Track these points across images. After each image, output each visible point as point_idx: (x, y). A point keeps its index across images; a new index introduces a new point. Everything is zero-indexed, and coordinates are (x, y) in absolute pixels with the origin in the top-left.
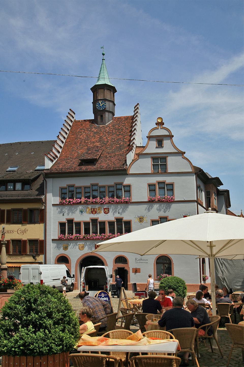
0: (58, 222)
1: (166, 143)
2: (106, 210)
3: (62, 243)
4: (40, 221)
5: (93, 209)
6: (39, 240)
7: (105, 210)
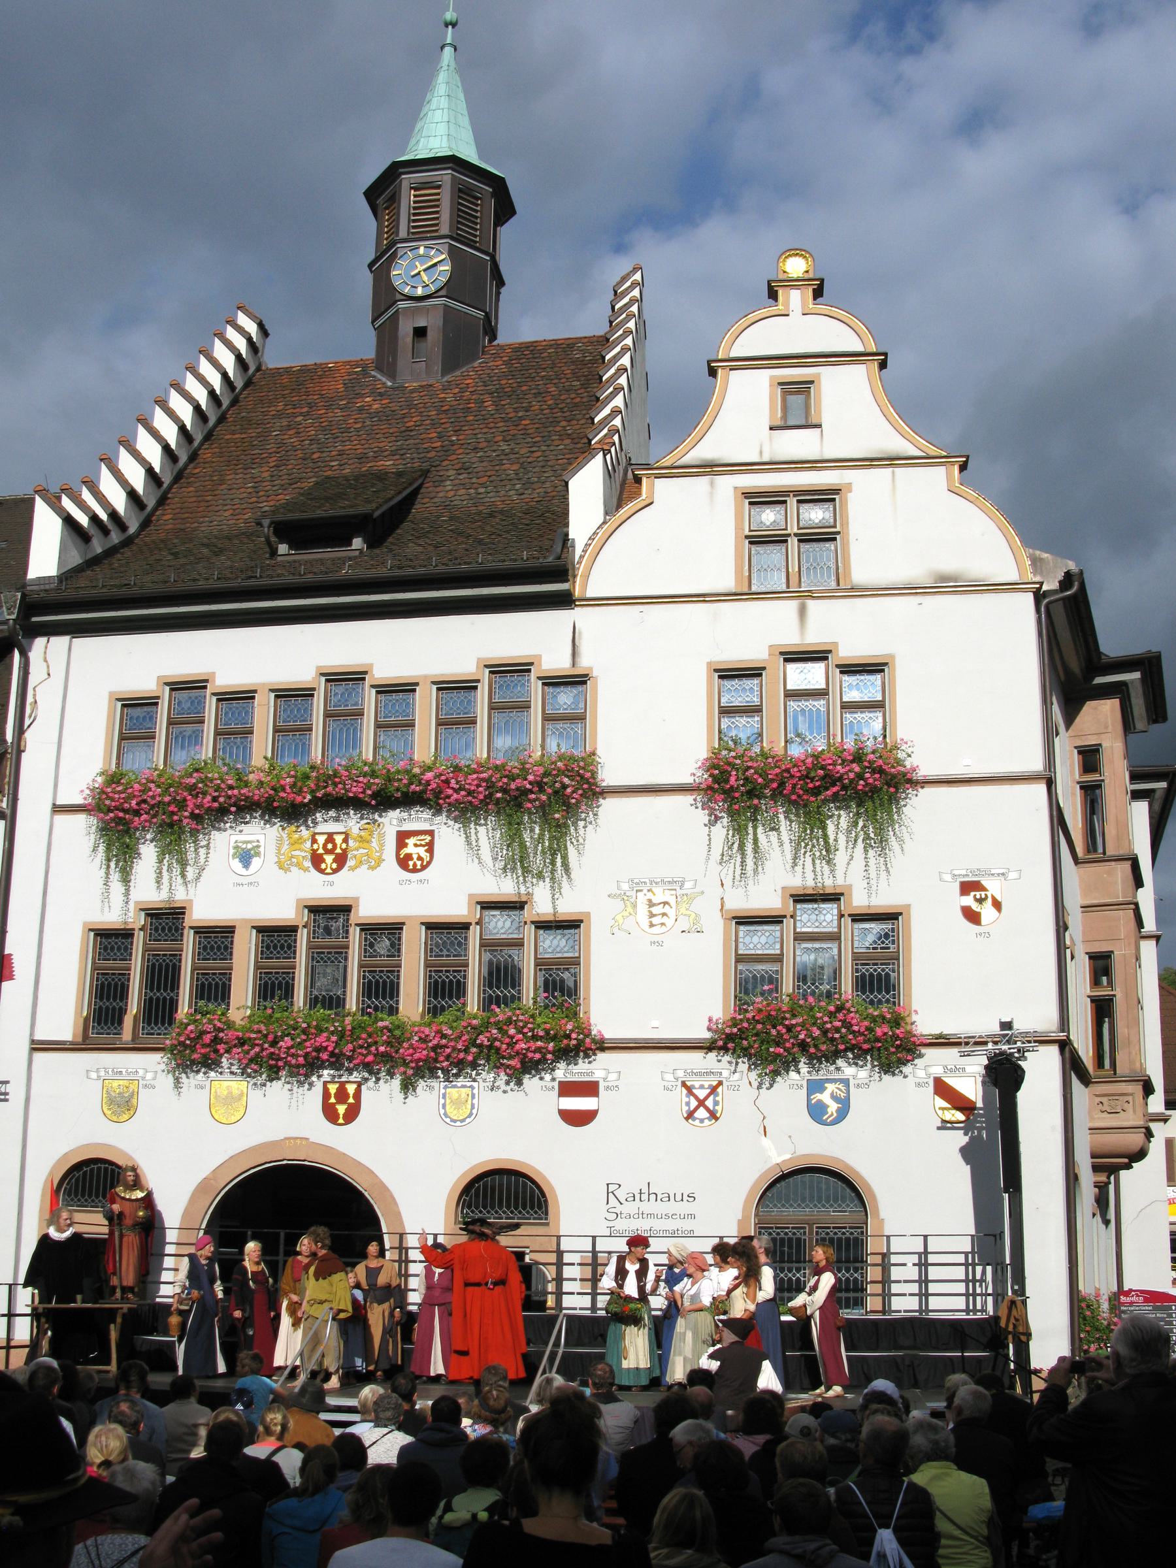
2: (411, 841)
5: (321, 839)
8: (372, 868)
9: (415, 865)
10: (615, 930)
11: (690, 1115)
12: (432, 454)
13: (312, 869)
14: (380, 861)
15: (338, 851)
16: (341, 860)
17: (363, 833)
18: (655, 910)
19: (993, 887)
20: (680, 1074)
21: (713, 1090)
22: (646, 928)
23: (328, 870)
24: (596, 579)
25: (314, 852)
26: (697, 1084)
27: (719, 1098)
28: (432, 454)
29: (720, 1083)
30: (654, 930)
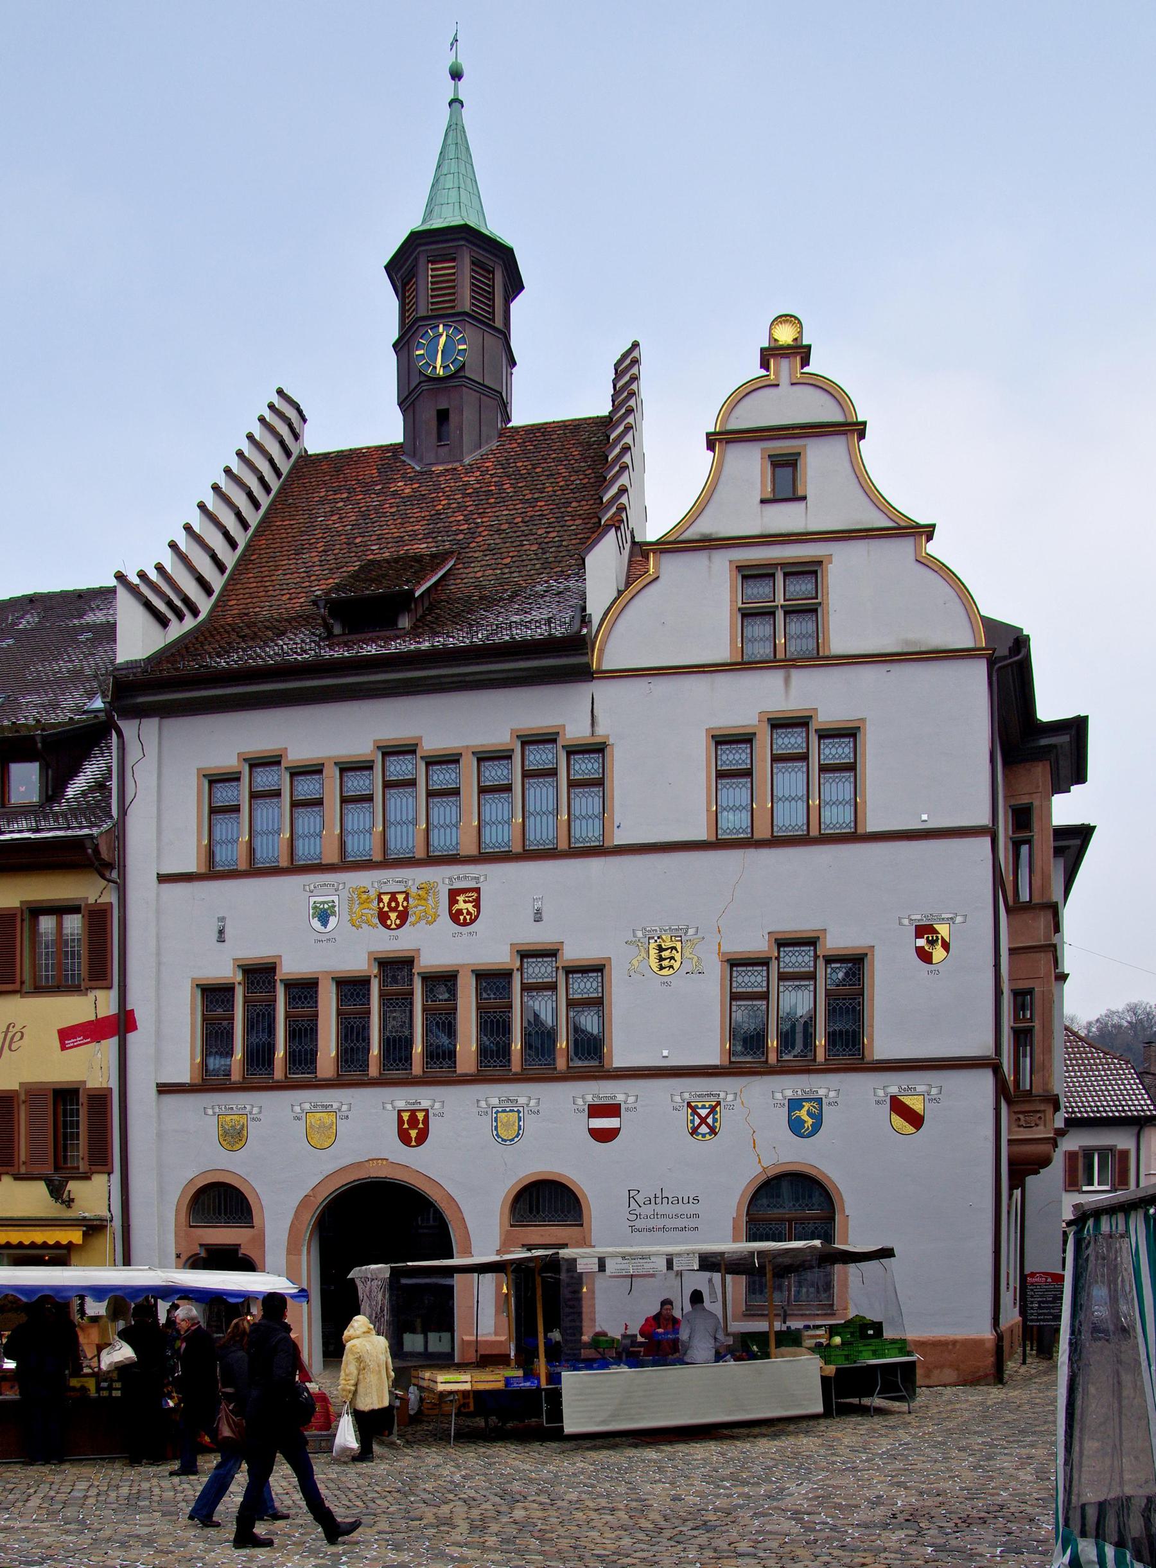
0: (193, 979)
1: (820, 461)
2: (461, 898)
3: (213, 1107)
4: (90, 973)
5: (386, 898)
6: (85, 1089)
7: (457, 902)
8: (429, 923)
9: (465, 919)
10: (632, 973)
11: (694, 1131)
12: (461, 537)
13: (379, 925)
14: (436, 916)
15: (401, 908)
16: (403, 916)
17: (420, 892)
18: (665, 954)
19: (943, 930)
20: (686, 1096)
21: (713, 1110)
22: (656, 969)
23: (393, 926)
24: (614, 652)
25: (381, 909)
26: (700, 1105)
27: (717, 1116)
28: (461, 537)
29: (719, 1103)
30: (665, 972)
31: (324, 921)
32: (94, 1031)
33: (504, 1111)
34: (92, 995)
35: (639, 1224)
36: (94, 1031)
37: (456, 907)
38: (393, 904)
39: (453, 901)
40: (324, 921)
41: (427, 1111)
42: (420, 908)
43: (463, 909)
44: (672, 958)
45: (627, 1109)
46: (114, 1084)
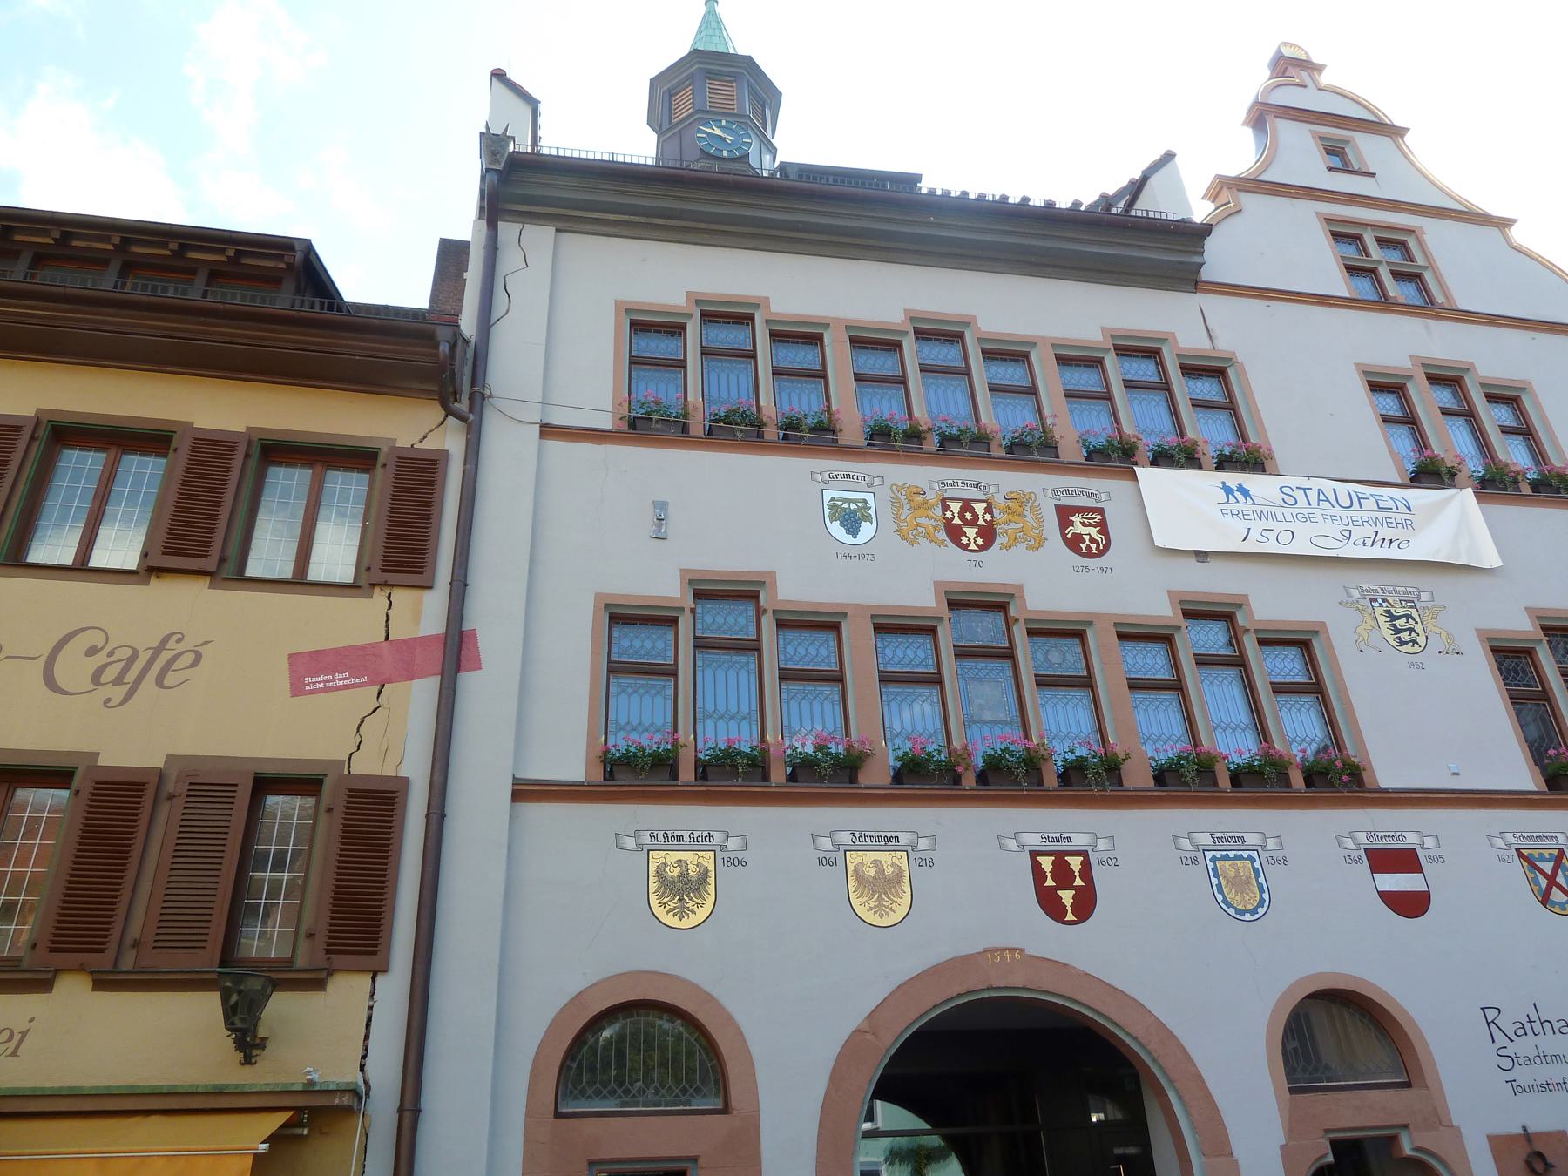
2: (1077, 519)
5: (956, 507)
8: (1035, 548)
9: (1088, 547)
13: (948, 542)
15: (981, 522)
17: (1011, 504)
18: (1401, 623)
20: (1510, 838)
23: (973, 547)
25: (948, 522)
26: (1535, 853)
30: (1408, 648)
31: (854, 531)
32: (378, 665)
33: (1225, 858)
34: (379, 597)
35: (1523, 1075)
36: (378, 665)
37: (1070, 531)
38: (968, 516)
39: (1064, 523)
40: (854, 531)
41: (1085, 854)
42: (1013, 525)
43: (1085, 535)
44: (1412, 630)
45: (1430, 859)
46: (415, 767)
